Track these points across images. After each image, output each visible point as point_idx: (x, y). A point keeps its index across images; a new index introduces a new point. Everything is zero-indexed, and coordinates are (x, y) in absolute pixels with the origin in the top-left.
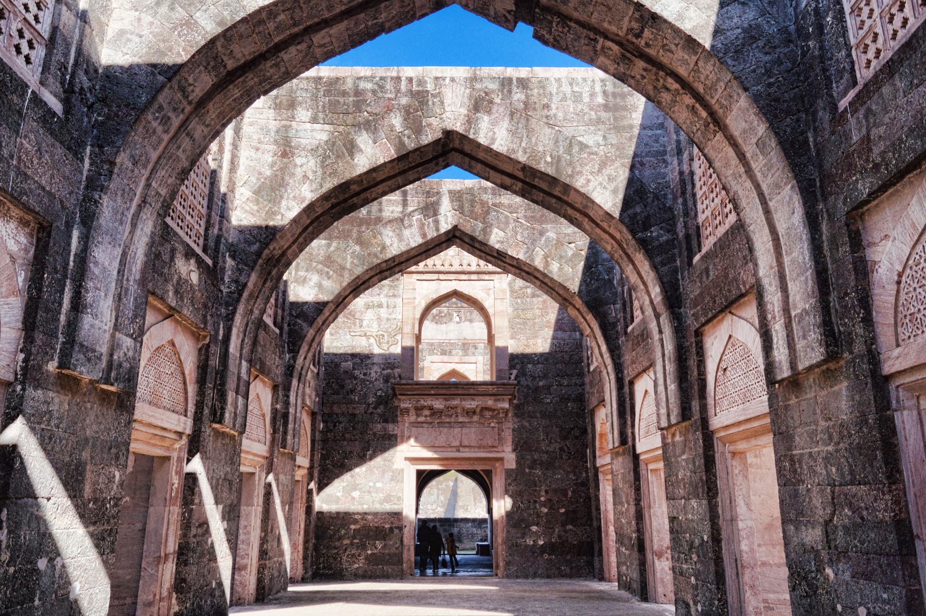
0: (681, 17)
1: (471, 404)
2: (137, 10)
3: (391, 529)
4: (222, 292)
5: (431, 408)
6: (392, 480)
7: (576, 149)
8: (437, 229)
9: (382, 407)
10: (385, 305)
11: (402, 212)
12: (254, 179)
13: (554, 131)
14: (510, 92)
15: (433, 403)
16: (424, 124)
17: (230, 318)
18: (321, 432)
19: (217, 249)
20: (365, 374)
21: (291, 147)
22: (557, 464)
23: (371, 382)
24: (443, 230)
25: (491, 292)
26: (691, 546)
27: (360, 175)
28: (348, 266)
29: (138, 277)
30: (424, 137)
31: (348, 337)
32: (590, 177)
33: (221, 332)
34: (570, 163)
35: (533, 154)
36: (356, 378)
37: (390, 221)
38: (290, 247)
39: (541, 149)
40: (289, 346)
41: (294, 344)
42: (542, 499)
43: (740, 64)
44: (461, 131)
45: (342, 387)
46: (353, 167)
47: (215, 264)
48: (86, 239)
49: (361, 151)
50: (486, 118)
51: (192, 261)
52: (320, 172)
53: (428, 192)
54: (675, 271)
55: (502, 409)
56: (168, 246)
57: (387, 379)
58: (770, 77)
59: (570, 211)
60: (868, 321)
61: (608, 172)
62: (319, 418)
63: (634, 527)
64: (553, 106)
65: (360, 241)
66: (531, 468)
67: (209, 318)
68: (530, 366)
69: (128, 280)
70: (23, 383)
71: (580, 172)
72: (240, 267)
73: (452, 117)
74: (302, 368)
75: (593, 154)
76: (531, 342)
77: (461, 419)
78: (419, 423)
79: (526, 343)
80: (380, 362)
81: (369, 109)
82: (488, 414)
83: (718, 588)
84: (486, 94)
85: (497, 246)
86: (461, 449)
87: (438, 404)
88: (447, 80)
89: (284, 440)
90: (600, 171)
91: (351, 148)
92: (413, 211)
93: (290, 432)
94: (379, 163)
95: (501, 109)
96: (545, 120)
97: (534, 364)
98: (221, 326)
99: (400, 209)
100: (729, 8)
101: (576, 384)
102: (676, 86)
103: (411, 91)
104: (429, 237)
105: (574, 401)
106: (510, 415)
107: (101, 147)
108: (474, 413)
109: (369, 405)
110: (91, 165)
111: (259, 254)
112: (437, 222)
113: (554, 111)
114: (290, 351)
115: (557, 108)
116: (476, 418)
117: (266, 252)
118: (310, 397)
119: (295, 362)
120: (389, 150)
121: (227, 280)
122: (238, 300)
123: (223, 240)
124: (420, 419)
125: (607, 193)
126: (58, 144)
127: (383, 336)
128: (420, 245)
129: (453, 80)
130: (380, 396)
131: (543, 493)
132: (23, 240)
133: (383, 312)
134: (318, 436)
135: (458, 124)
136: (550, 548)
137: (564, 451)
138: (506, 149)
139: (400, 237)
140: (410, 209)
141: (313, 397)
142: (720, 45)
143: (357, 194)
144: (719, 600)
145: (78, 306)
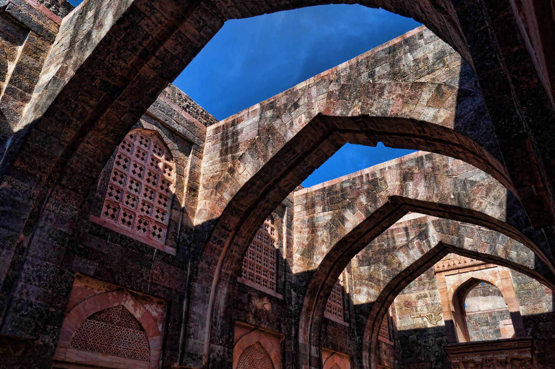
0: (435, 117)
1: (502, 357)
4: (291, 311)
5: (473, 362)
7: (468, 186)
8: (430, 246)
9: (440, 363)
10: (429, 295)
11: (407, 241)
12: (300, 248)
13: (452, 179)
14: (423, 164)
16: (378, 196)
17: (297, 324)
20: (425, 342)
21: (315, 227)
24: (433, 246)
25: (498, 275)
27: (349, 233)
28: (382, 279)
29: (222, 315)
30: (378, 204)
31: (410, 319)
32: (481, 200)
33: (293, 332)
34: (467, 195)
35: (443, 196)
36: (420, 345)
37: (401, 248)
38: (326, 279)
39: (446, 192)
40: (357, 332)
41: (360, 331)
43: (475, 131)
44: (398, 195)
45: (413, 352)
46: (345, 230)
48: (188, 304)
49: (348, 220)
50: (411, 183)
53: (420, 225)
55: (527, 358)
56: (246, 296)
57: (440, 344)
59: (484, 223)
61: (493, 194)
64: (450, 164)
65: (386, 263)
67: (282, 326)
68: (541, 324)
69: (215, 318)
71: (475, 199)
73: (392, 188)
74: (370, 344)
75: (480, 186)
76: (537, 306)
79: (533, 307)
80: (433, 333)
81: (349, 197)
82: (517, 363)
84: (409, 169)
87: (478, 359)
88: (387, 169)
90: (487, 195)
91: (343, 220)
92: (413, 238)
94: (357, 224)
95: (419, 176)
96: (446, 174)
97: (544, 322)
98: (293, 329)
99: (405, 239)
100: (464, 102)
103: (369, 181)
104: (425, 252)
106: (535, 362)
107: (193, 262)
108: (506, 363)
109: (432, 362)
111: (306, 287)
112: (428, 242)
113: (451, 167)
114: (358, 335)
115: (452, 165)
117: (310, 285)
118: (388, 361)
119: (362, 341)
120: (361, 216)
121: (293, 303)
122: (299, 314)
125: (495, 208)
126: (172, 267)
127: (431, 315)
128: (421, 258)
129: (390, 168)
132: (160, 310)
133: (428, 300)
135: (396, 191)
138: (425, 197)
139: (408, 256)
140: (411, 237)
141: (392, 361)
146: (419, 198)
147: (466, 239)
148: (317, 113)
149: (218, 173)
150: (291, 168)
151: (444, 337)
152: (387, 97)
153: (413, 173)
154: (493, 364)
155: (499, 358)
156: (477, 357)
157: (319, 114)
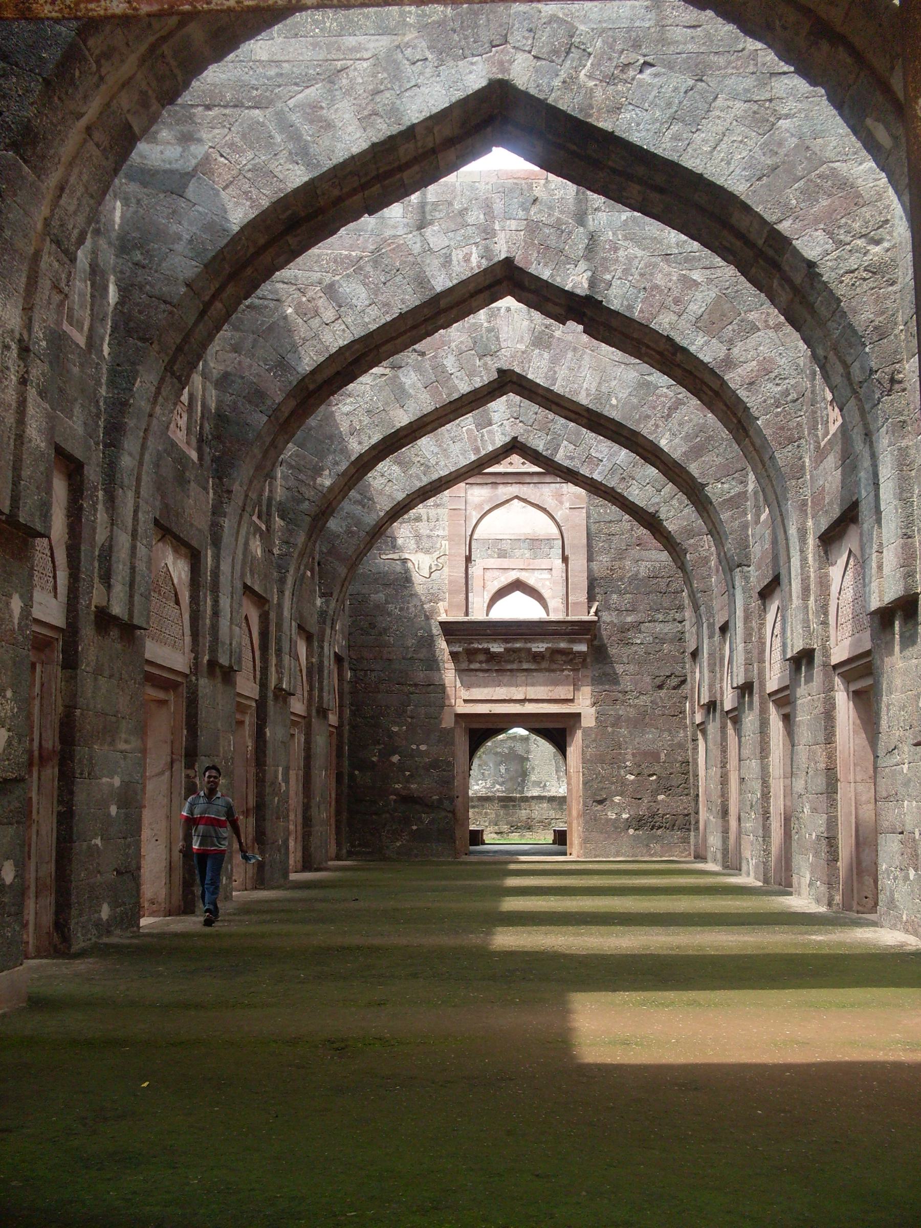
1: (539, 647)
2: (236, 352)
3: (440, 801)
5: (487, 651)
6: (439, 741)
8: (493, 443)
15: (490, 646)
17: (282, 581)
18: (350, 682)
19: (269, 514)
20: (401, 609)
22: (647, 720)
23: (409, 619)
24: (499, 444)
25: (565, 498)
26: (752, 806)
36: (390, 614)
40: (320, 589)
42: (628, 763)
45: (372, 626)
47: (268, 528)
51: (257, 536)
52: (366, 420)
54: (745, 526)
58: (777, 407)
59: (640, 450)
60: (825, 623)
62: (346, 665)
63: (719, 793)
66: (613, 726)
68: (615, 596)
70: (196, 675)
71: (648, 417)
72: (290, 527)
73: (508, 354)
76: (617, 564)
77: (525, 666)
78: (472, 670)
79: (609, 564)
82: (559, 657)
83: (764, 841)
85: (566, 463)
86: (527, 704)
88: (503, 311)
89: (321, 697)
90: (669, 416)
93: (326, 688)
97: (620, 593)
101: (675, 620)
102: (710, 393)
104: (483, 453)
105: (672, 641)
107: (220, 478)
110: (214, 494)
114: (323, 595)
116: (544, 665)
119: (328, 607)
123: (274, 503)
124: (472, 666)
130: (422, 637)
131: (629, 757)
134: (347, 688)
136: (639, 822)
137: (657, 704)
142: (737, 378)
143: (406, 436)
144: (764, 851)
145: (216, 614)
146: (556, 388)
147: (565, 442)
148: (503, 256)
149: (266, 303)
150: (414, 327)
151: (441, 604)
152: (638, 281)
153: (552, 336)
154: (519, 658)
155: (533, 650)
156: (495, 645)
157: (507, 258)
